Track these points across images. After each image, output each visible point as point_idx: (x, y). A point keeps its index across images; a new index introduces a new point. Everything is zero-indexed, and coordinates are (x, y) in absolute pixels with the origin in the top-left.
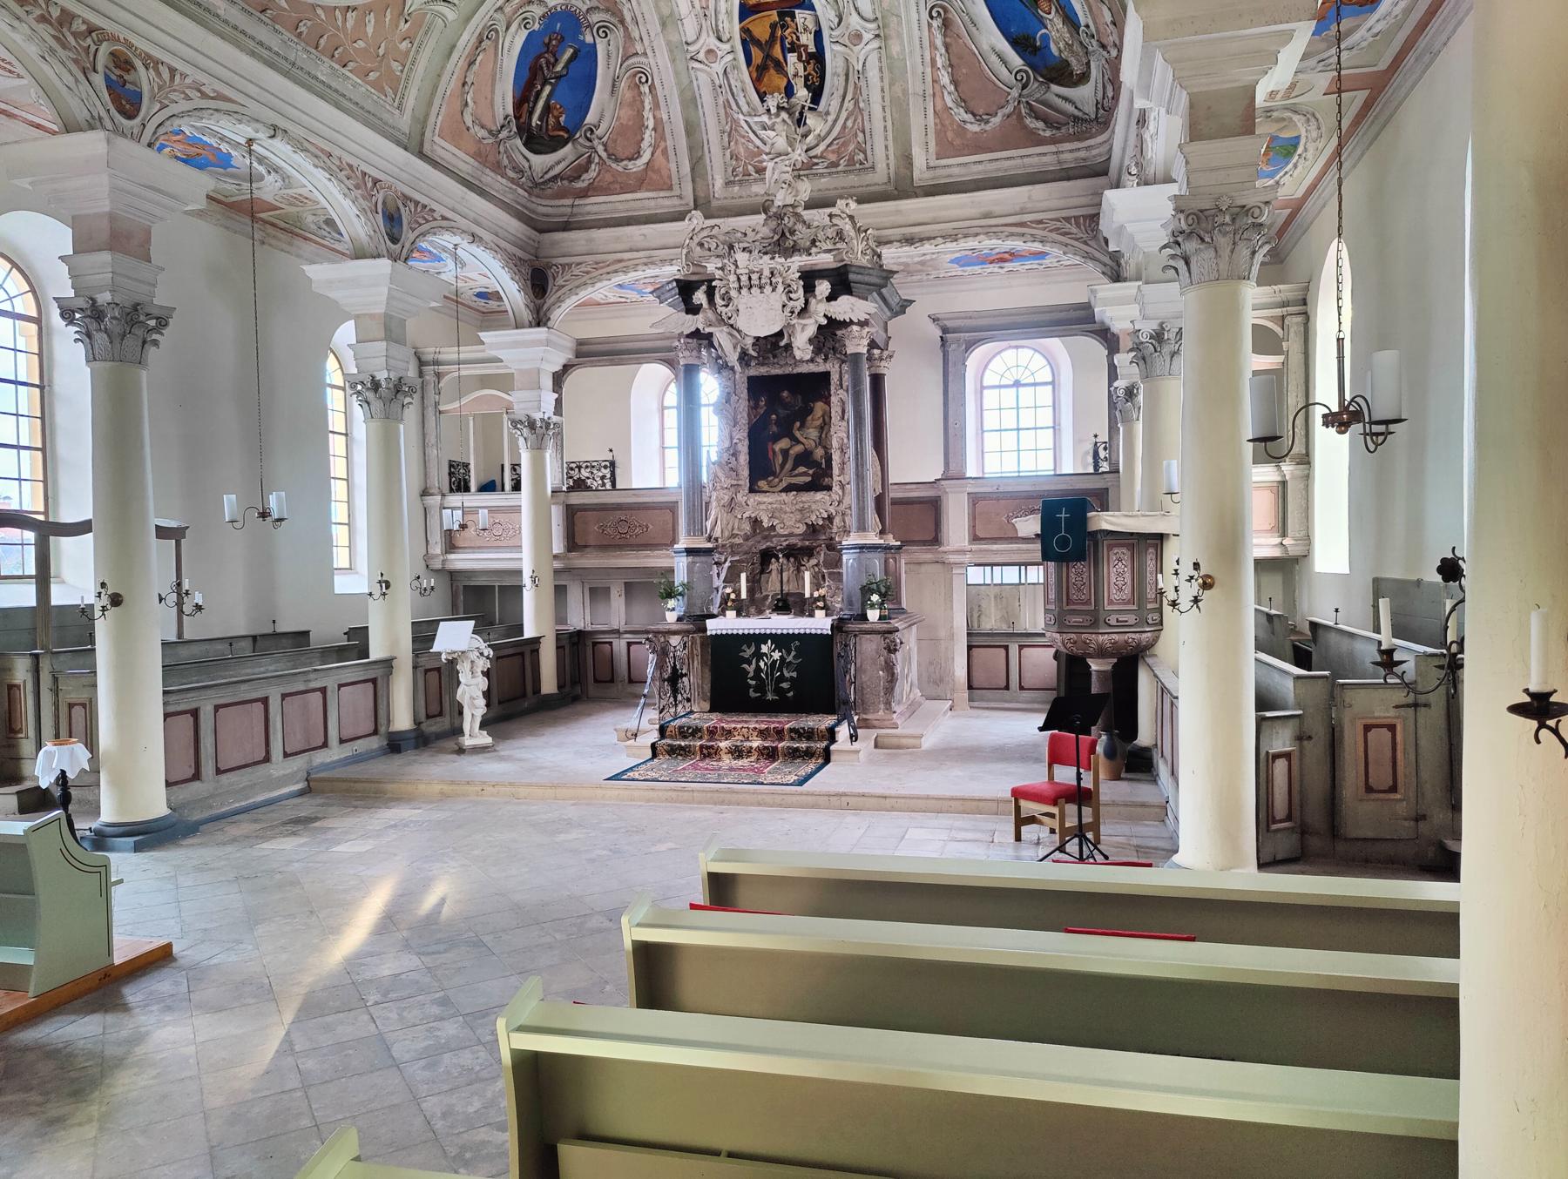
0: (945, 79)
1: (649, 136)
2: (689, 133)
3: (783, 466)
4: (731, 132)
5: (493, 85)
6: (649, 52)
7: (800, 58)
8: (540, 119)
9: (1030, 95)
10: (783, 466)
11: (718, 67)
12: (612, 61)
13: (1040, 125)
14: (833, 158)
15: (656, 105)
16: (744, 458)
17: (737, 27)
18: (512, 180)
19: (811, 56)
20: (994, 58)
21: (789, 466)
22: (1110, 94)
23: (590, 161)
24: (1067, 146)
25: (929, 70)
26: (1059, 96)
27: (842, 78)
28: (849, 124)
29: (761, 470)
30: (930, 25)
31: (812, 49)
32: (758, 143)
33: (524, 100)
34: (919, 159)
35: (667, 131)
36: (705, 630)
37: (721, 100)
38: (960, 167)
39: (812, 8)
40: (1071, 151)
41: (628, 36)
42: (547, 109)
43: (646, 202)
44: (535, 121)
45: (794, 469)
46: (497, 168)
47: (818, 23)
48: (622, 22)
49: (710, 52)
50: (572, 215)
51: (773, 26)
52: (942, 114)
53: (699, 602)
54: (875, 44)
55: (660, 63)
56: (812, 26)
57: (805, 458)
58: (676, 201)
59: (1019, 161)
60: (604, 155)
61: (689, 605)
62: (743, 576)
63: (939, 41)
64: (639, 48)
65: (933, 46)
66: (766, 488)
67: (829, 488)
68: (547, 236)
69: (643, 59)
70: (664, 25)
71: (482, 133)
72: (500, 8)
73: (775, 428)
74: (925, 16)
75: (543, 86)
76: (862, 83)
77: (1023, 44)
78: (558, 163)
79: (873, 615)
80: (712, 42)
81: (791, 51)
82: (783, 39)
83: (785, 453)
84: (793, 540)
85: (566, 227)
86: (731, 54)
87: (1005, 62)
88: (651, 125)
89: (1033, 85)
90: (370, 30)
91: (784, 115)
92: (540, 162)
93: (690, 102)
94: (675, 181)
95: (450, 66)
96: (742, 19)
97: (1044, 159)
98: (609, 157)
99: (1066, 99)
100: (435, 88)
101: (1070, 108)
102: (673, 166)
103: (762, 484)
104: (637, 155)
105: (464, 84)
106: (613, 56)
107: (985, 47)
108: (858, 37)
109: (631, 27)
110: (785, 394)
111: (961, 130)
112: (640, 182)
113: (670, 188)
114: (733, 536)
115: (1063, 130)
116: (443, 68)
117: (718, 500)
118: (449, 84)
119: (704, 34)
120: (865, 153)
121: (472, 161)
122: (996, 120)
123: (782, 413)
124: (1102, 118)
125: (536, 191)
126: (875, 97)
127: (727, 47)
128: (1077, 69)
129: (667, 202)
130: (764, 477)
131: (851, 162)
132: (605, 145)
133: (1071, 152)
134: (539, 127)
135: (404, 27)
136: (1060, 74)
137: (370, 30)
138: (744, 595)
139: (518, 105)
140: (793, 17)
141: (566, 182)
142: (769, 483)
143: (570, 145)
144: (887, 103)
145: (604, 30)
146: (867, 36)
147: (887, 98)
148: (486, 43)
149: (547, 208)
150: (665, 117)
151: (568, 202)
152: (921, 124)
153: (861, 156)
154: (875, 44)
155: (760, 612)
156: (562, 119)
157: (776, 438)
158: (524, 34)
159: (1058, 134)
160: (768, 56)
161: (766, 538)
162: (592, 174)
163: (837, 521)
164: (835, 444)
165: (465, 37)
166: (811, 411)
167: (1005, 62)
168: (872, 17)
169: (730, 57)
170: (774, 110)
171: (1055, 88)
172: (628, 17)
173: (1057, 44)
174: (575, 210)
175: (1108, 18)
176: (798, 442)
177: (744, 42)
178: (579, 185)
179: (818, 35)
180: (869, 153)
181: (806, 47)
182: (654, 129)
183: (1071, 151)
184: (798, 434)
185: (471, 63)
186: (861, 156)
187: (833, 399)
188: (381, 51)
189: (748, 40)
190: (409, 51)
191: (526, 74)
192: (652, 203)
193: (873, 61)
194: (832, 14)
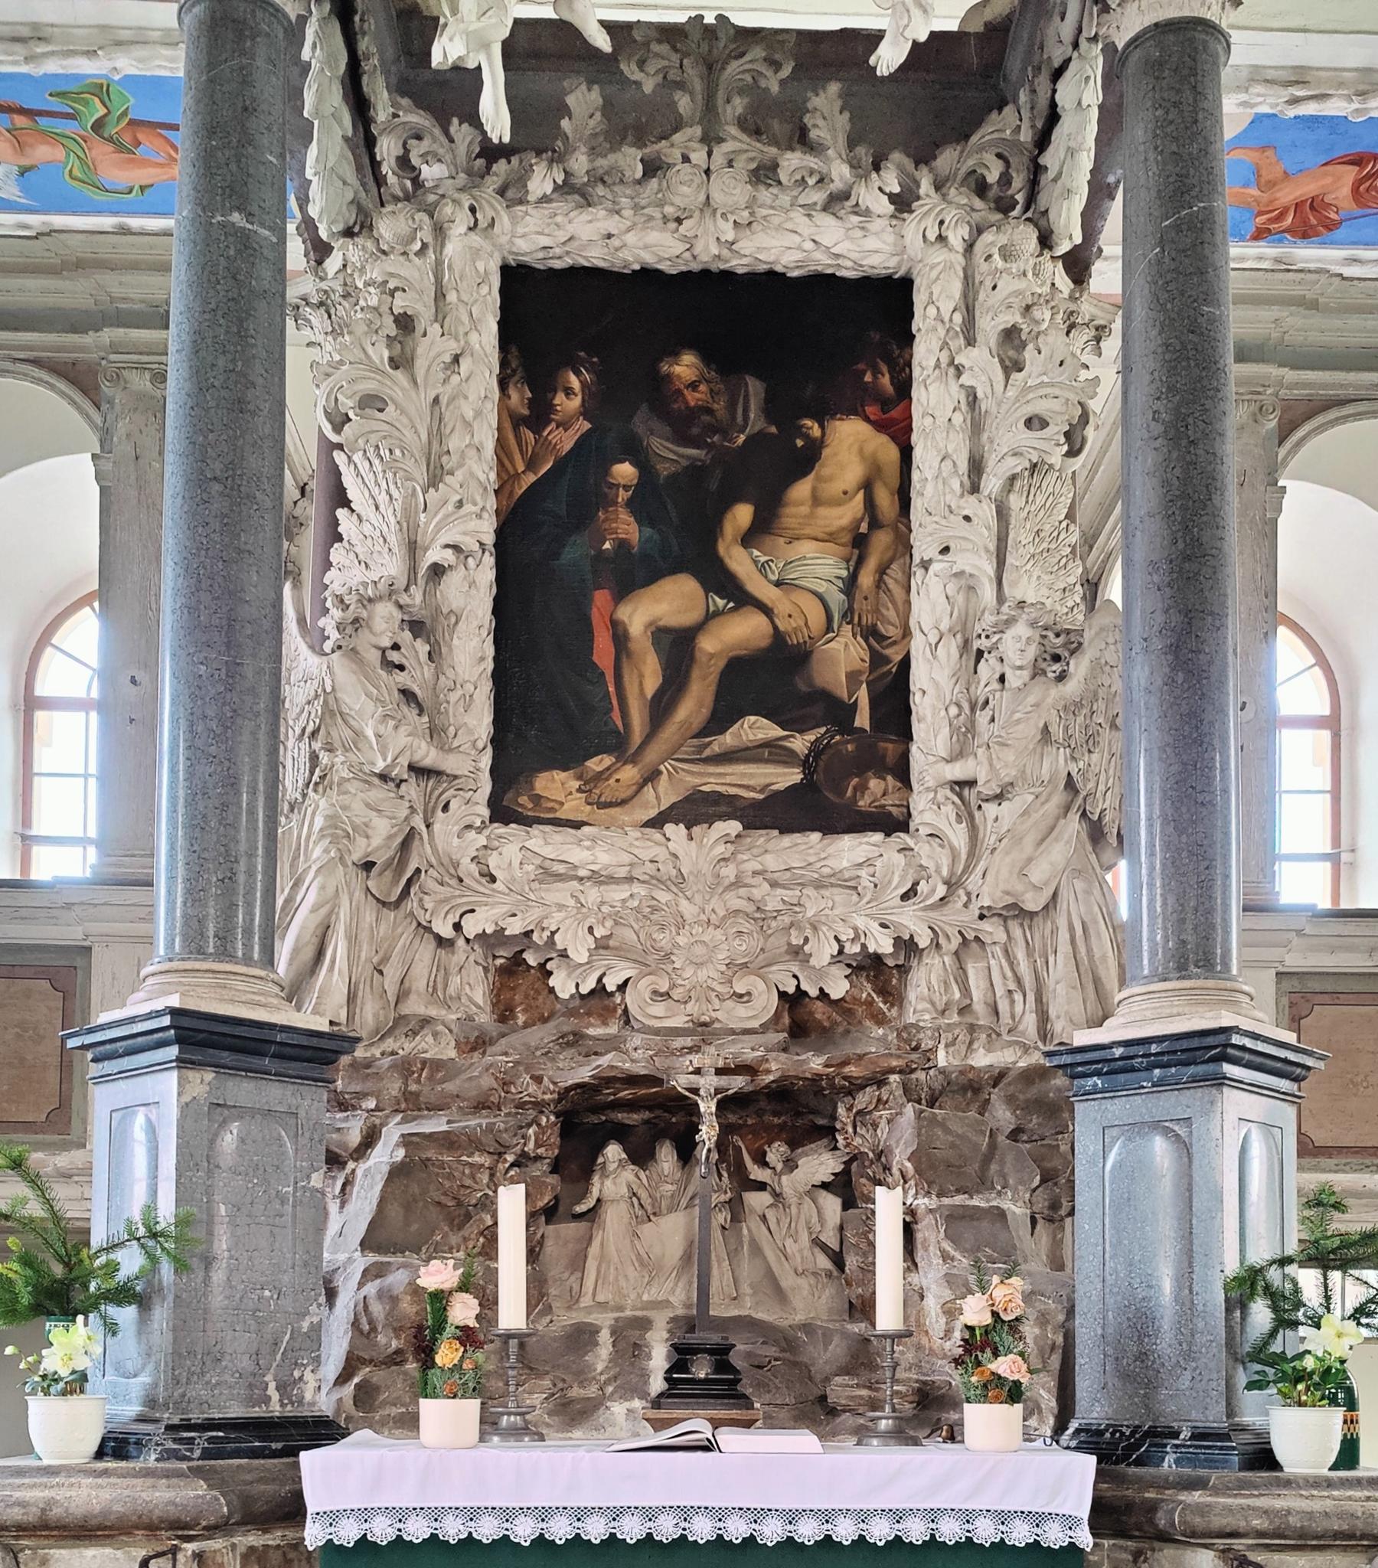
3: (661, 707)
10: (661, 707)
16: (472, 650)
21: (693, 706)
29: (548, 718)
36: (293, 1511)
45: (720, 719)
53: (239, 1347)
57: (771, 679)
61: (187, 1356)
62: (512, 1205)
66: (574, 806)
67: (893, 823)
73: (626, 527)
79: (1302, 1436)
83: (677, 646)
84: (747, 1051)
103: (556, 786)
110: (685, 367)
114: (404, 1025)
117: (338, 832)
123: (670, 454)
130: (568, 758)
138: (512, 1314)
142: (590, 783)
155: (574, 1413)
157: (633, 574)
161: (573, 1040)
163: (925, 987)
164: (930, 605)
166: (807, 459)
176: (741, 598)
184: (739, 561)
187: (933, 401)
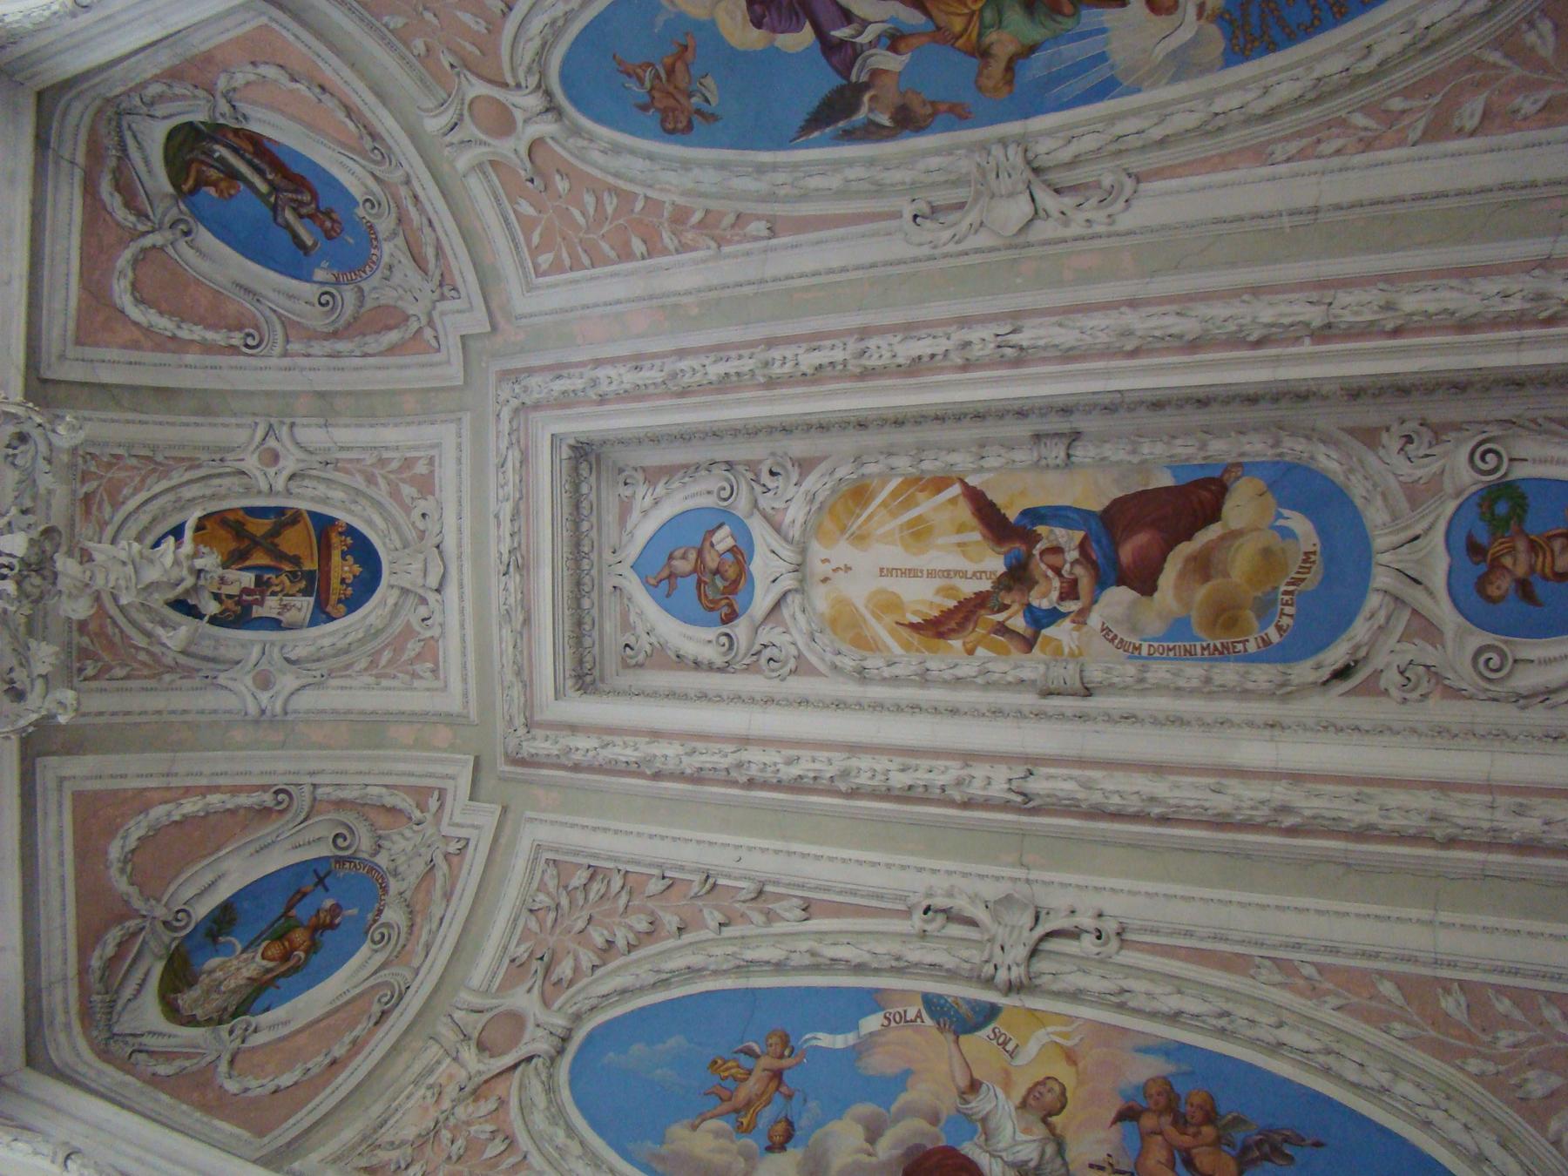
0: (191, 806)
1: (164, 324)
2: (158, 391)
4: (153, 463)
5: (300, 121)
6: (286, 361)
7: (246, 591)
8: (221, 160)
9: (153, 931)
11: (251, 463)
12: (282, 300)
13: (110, 950)
14: (92, 627)
15: (208, 348)
17: (303, 505)
18: (144, 85)
19: (247, 608)
20: (208, 877)
22: (163, 1069)
23: (142, 215)
24: (74, 993)
25: (204, 782)
26: (147, 974)
27: (209, 653)
28: (142, 656)
30: (264, 788)
31: (257, 611)
32: (132, 505)
33: (260, 150)
34: (80, 768)
35: (167, 357)
37: (204, 456)
38: (58, 827)
39: (313, 622)
40: (66, 1001)
41: (313, 336)
42: (233, 175)
43: (65, 296)
44: (221, 151)
46: (172, 75)
47: (291, 627)
48: (335, 335)
49: (275, 457)
50: (58, 158)
51: (296, 560)
52: (140, 801)
54: (253, 709)
55: (263, 373)
56: (287, 617)
58: (56, 348)
59: (57, 922)
60: (148, 241)
63: (243, 800)
64: (295, 347)
65: (235, 790)
68: (32, 100)
69: (278, 350)
70: (322, 395)
71: (240, 79)
72: (408, 182)
74: (280, 782)
75: (270, 183)
76: (197, 682)
77: (224, 919)
78: (147, 162)
80: (289, 464)
81: (258, 580)
82: (277, 571)
85: (42, 142)
86: (268, 486)
87: (200, 895)
88: (180, 334)
89: (167, 936)
90: (467, 18)
91: (190, 581)
92: (156, 134)
93: (206, 404)
94: (90, 352)
95: (360, 86)
96: (312, 514)
97: (57, 962)
98: (144, 250)
99: (141, 986)
100: (338, 52)
101: (128, 992)
102: (114, 354)
104: (140, 301)
105: (323, 88)
106: (289, 304)
107: (225, 866)
108: (265, 682)
109: (328, 346)
111: (111, 832)
112: (95, 292)
113: (79, 342)
115: (98, 986)
116: (362, 75)
118: (333, 70)
119: (303, 456)
120: (95, 678)
121: (205, 47)
122: (122, 885)
124: (114, 1046)
125: (110, 112)
126: (178, 701)
127: (280, 484)
128: (185, 1000)
129: (56, 332)
131: (85, 654)
132: (162, 249)
133: (62, 1000)
134: (209, 153)
135: (446, 60)
136: (179, 974)
137: (467, 18)
139: (256, 140)
140: (306, 592)
141: (113, 163)
143: (170, 189)
144: (166, 717)
145: (326, 302)
146: (264, 697)
147: (173, 718)
148: (368, 143)
149: (77, 116)
150: (189, 358)
151: (80, 158)
152: (130, 770)
153: (90, 672)
154: (253, 709)
156: (212, 191)
158: (357, 192)
159: (93, 978)
160: (255, 543)
162: (121, 213)
165: (390, 122)
167: (200, 895)
168: (290, 707)
169: (264, 486)
170: (199, 563)
171: (159, 968)
172: (341, 346)
173: (221, 967)
174: (65, 164)
175: (286, 1080)
177: (280, 511)
178: (106, 187)
179: (275, 624)
180: (94, 684)
181: (261, 603)
182: (174, 338)
183: (66, 1001)
185: (349, 111)
186: (90, 672)
188: (428, 16)
189: (285, 518)
190: (406, 44)
191: (296, 169)
192: (58, 306)
193: (231, 702)
194: (300, 652)
